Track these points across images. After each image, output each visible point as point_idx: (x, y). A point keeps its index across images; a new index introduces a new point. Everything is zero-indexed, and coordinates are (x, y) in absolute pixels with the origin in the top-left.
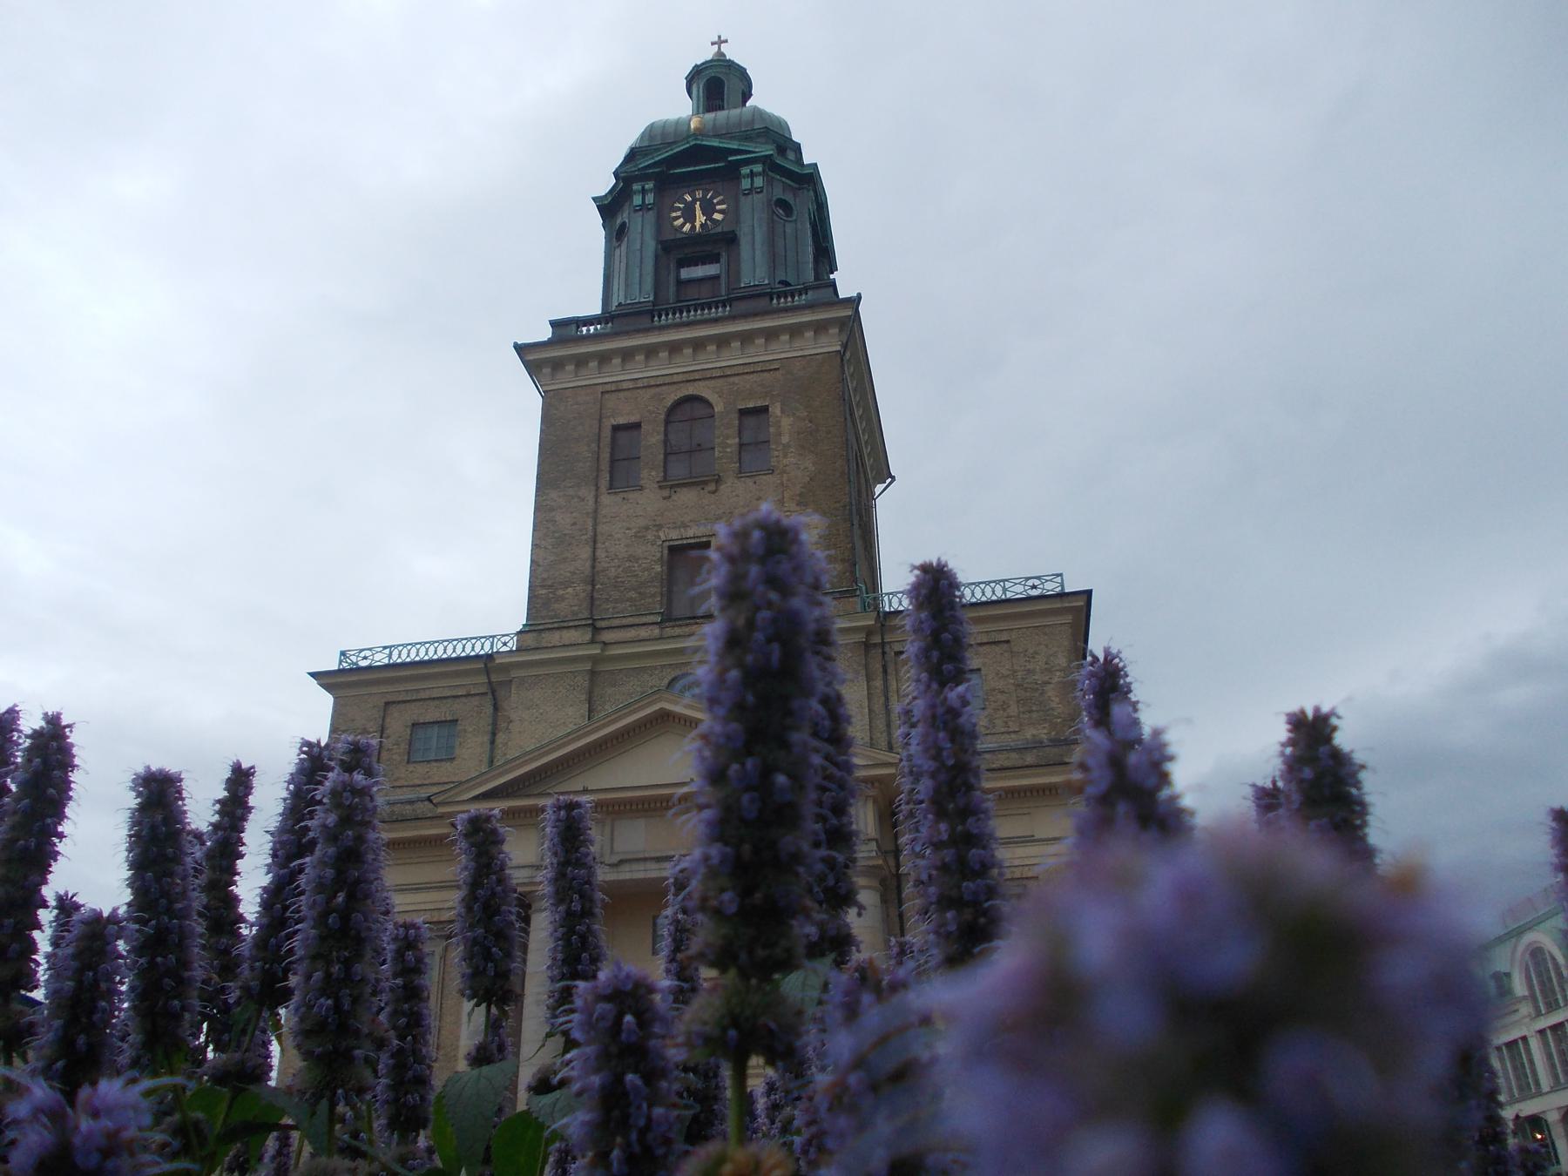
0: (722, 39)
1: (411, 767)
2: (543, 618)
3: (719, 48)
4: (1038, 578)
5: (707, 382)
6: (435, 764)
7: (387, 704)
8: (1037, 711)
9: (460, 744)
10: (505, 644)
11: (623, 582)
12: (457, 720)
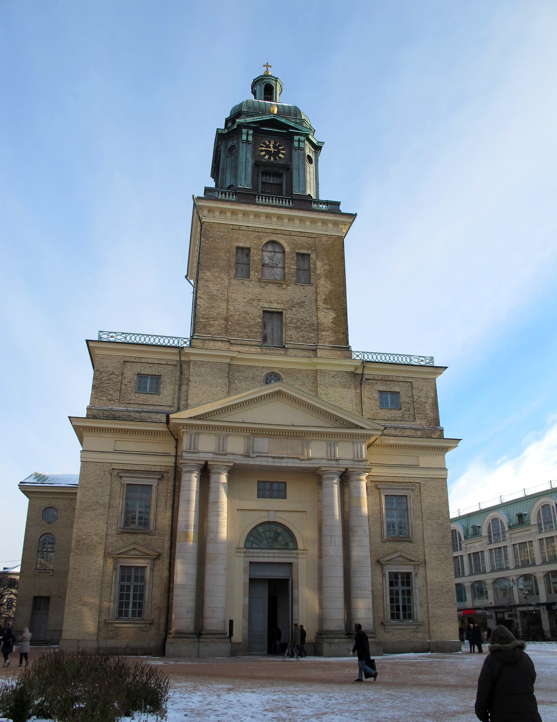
1: (137, 395)
2: (204, 333)
3: (267, 69)
4: (424, 357)
5: (281, 236)
6: (150, 396)
7: (124, 361)
8: (422, 414)
9: (163, 388)
10: (185, 343)
11: (242, 323)
12: (161, 376)
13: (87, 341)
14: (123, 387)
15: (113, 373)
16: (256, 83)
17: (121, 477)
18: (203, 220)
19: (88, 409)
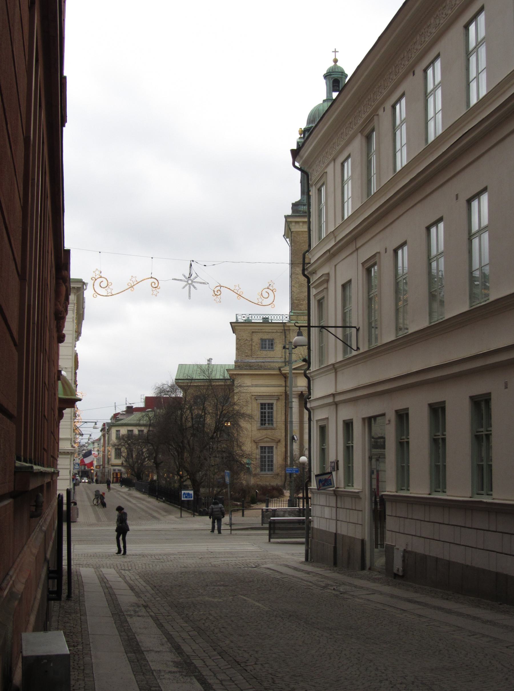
0: (336, 50)
1: (261, 352)
2: (297, 310)
10: (286, 317)
13: (231, 323)
14: (253, 348)
15: (247, 340)
16: (326, 76)
17: (257, 400)
18: (292, 230)
19: (236, 362)
